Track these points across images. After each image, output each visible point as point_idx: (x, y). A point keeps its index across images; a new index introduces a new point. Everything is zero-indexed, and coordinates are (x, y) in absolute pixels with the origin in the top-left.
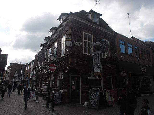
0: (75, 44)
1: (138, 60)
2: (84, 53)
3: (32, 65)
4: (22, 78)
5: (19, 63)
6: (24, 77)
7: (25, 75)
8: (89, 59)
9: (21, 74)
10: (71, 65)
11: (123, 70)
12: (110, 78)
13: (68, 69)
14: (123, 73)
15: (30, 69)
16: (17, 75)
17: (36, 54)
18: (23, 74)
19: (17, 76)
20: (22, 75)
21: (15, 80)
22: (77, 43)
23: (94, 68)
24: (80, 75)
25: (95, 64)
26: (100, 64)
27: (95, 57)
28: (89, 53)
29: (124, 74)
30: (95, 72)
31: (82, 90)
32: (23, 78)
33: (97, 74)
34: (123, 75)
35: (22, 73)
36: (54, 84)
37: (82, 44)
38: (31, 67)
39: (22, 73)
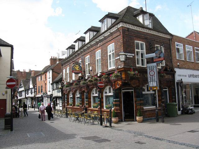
0: (127, 56)
2: (137, 65)
3: (50, 75)
4: (33, 93)
5: (22, 70)
8: (143, 71)
10: (124, 80)
12: (167, 91)
13: (120, 84)
16: (23, 89)
17: (52, 57)
18: (34, 87)
19: (23, 91)
20: (33, 90)
22: (129, 54)
24: (133, 90)
25: (150, 77)
26: (156, 77)
28: (143, 64)
31: (137, 106)
32: (34, 93)
35: (31, 86)
36: (88, 101)
37: (134, 55)
39: (31, 86)
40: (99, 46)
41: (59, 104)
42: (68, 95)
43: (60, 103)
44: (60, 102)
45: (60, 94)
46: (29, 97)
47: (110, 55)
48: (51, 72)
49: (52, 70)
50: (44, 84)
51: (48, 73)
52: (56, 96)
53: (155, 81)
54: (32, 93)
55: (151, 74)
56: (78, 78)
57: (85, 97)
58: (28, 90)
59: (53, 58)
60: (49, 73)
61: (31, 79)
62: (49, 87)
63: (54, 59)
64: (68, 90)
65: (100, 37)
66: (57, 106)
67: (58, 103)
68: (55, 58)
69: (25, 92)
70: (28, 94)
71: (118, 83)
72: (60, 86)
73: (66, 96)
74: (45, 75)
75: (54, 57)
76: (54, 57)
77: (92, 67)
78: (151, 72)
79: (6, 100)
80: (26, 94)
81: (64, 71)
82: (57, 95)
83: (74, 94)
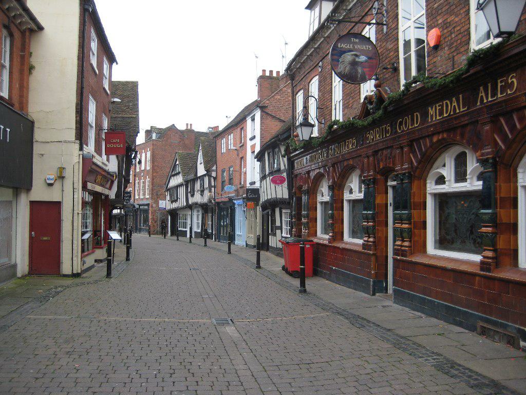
4: (207, 193)
5: (181, 127)
6: (213, 189)
7: (215, 179)
9: (199, 174)
15: (243, 146)
17: (264, 71)
19: (180, 185)
20: (206, 179)
21: (173, 201)
32: (210, 191)
35: (201, 171)
38: (249, 136)
39: (201, 171)
41: (281, 228)
42: (313, 192)
43: (284, 227)
44: (283, 219)
45: (282, 192)
46: (196, 204)
48: (258, 114)
49: (263, 108)
50: (238, 161)
51: (249, 120)
52: (269, 197)
54: (202, 192)
56: (357, 110)
57: (390, 199)
58: (194, 180)
59: (268, 74)
60: (253, 120)
61: (201, 148)
62: (252, 172)
63: (271, 77)
64: (312, 174)
66: (275, 235)
67: (278, 224)
68: (275, 75)
69: (187, 188)
70: (193, 196)
72: (283, 163)
73: (304, 198)
74: (239, 129)
75: (271, 72)
76: (271, 72)
77: (445, 26)
79: (57, 205)
80: (189, 195)
81: (300, 98)
82: (274, 196)
83: (337, 188)
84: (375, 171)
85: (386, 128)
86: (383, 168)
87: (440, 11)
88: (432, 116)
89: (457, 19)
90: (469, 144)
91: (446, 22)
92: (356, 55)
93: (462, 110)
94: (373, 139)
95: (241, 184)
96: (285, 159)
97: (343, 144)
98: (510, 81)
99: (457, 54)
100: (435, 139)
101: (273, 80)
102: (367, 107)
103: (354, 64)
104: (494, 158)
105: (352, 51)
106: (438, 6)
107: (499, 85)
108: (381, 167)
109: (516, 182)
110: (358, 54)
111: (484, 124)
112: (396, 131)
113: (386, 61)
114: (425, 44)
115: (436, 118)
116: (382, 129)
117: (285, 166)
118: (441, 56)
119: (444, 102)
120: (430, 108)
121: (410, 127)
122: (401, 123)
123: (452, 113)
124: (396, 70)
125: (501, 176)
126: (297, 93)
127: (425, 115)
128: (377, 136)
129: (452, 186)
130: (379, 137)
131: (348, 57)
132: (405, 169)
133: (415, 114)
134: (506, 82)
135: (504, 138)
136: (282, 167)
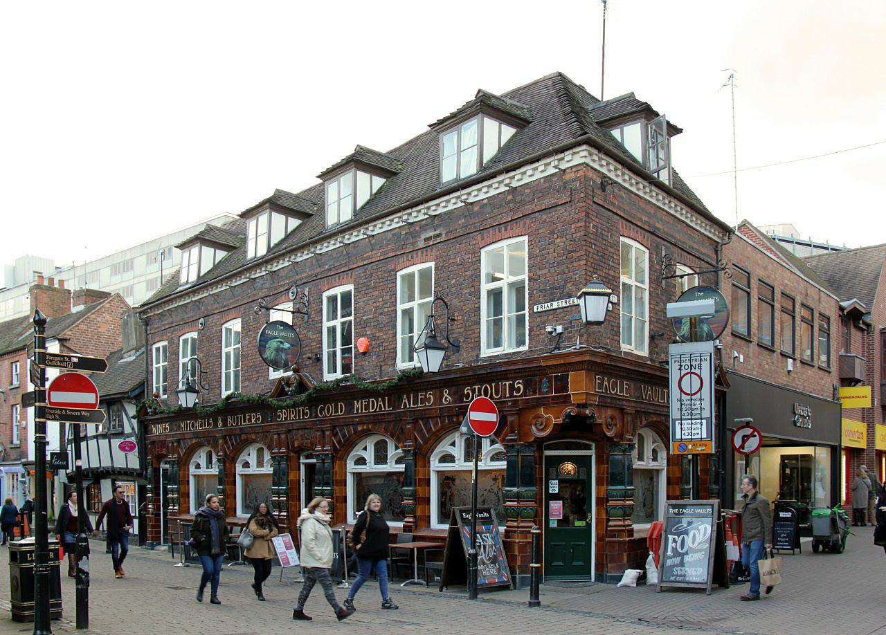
1: (790, 368)
2: (624, 347)
10: (578, 406)
11: (747, 425)
14: (745, 439)
23: (677, 422)
27: (680, 369)
29: (746, 445)
30: (678, 436)
33: (690, 447)
34: (742, 447)
40: (421, 244)
45: (134, 462)
47: (496, 295)
53: (701, 419)
55: (686, 389)
65: (438, 205)
71: (539, 416)
77: (373, 338)
78: (686, 379)
84: (288, 448)
85: (303, 410)
86: (298, 446)
87: (369, 324)
88: (358, 409)
89: (385, 337)
90: (392, 436)
91: (374, 335)
92: (281, 343)
93: (387, 409)
94: (286, 419)
95: (12, 442)
96: (135, 422)
97: (241, 417)
98: (428, 396)
99: (385, 365)
100: (360, 428)
101: (55, 293)
102: (283, 388)
103: (278, 350)
104: (414, 450)
105: (277, 338)
106: (367, 319)
107: (420, 397)
108: (296, 445)
109: (429, 467)
110: (283, 341)
111: (408, 423)
112: (317, 416)
113: (307, 349)
114: (353, 346)
115: (362, 410)
116: (299, 411)
117: (133, 429)
118: (369, 362)
119: (371, 400)
120: (355, 402)
121: (333, 414)
122: (322, 409)
123: (378, 410)
124: (319, 360)
125: (419, 463)
126: (155, 343)
127: (350, 407)
128: (292, 416)
129: (371, 467)
130: (295, 417)
131: (273, 344)
132: (326, 450)
133: (339, 404)
134: (425, 396)
135: (423, 437)
136: (128, 430)
